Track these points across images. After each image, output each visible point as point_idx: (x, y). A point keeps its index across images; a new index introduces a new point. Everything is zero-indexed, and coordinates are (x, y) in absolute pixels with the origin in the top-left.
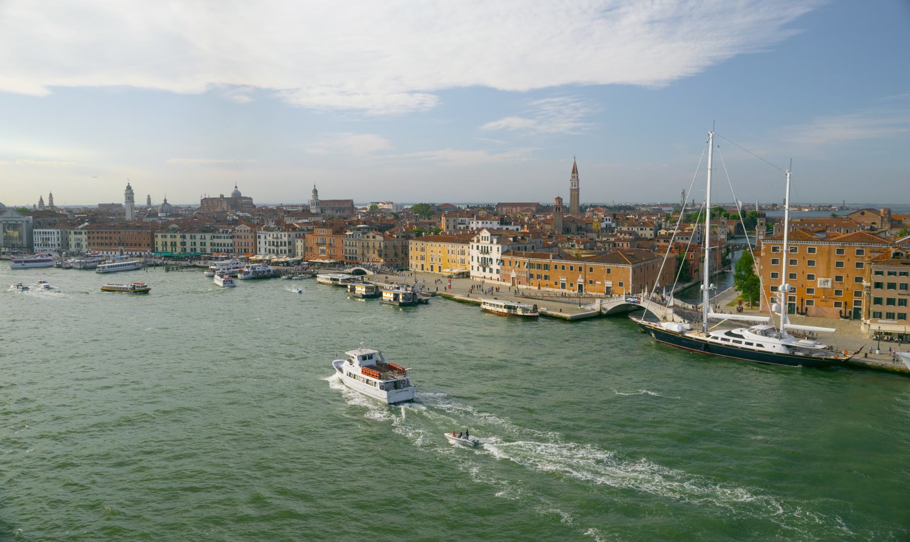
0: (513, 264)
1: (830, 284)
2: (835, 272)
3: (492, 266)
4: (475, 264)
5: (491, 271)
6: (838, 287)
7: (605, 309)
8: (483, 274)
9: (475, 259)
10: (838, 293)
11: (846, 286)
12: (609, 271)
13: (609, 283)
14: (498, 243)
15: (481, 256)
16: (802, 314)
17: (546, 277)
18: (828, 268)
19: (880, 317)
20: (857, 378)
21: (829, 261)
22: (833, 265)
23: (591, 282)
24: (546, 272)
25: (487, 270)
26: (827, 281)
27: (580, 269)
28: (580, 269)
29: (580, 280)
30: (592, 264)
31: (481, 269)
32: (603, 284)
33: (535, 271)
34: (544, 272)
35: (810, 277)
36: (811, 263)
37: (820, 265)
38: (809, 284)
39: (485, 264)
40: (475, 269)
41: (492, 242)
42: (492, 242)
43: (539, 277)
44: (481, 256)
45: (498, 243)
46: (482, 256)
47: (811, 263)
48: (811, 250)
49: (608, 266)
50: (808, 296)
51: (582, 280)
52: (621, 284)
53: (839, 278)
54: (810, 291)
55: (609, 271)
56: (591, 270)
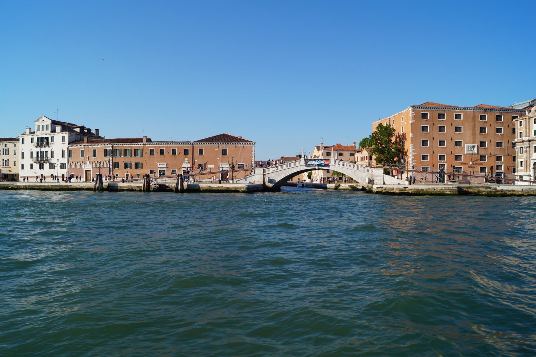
0: (86, 155)
1: (475, 149)
2: (480, 138)
3: (53, 161)
4: (28, 161)
5: (52, 166)
6: (483, 153)
7: (270, 181)
8: (39, 172)
9: (27, 155)
10: (483, 158)
11: (490, 151)
12: (225, 152)
14: (62, 131)
15: (35, 150)
17: (137, 166)
18: (474, 134)
21: (474, 127)
22: (478, 131)
24: (138, 159)
25: (46, 166)
26: (473, 147)
27: (186, 152)
28: (186, 152)
31: (36, 166)
33: (120, 160)
34: (133, 160)
35: (458, 143)
37: (466, 132)
38: (457, 151)
39: (41, 160)
40: (27, 167)
41: (53, 131)
42: (53, 131)
43: (126, 166)
44: (35, 150)
45: (62, 131)
46: (38, 149)
50: (457, 163)
53: (483, 144)
54: (458, 157)
55: (225, 152)
56: (201, 151)
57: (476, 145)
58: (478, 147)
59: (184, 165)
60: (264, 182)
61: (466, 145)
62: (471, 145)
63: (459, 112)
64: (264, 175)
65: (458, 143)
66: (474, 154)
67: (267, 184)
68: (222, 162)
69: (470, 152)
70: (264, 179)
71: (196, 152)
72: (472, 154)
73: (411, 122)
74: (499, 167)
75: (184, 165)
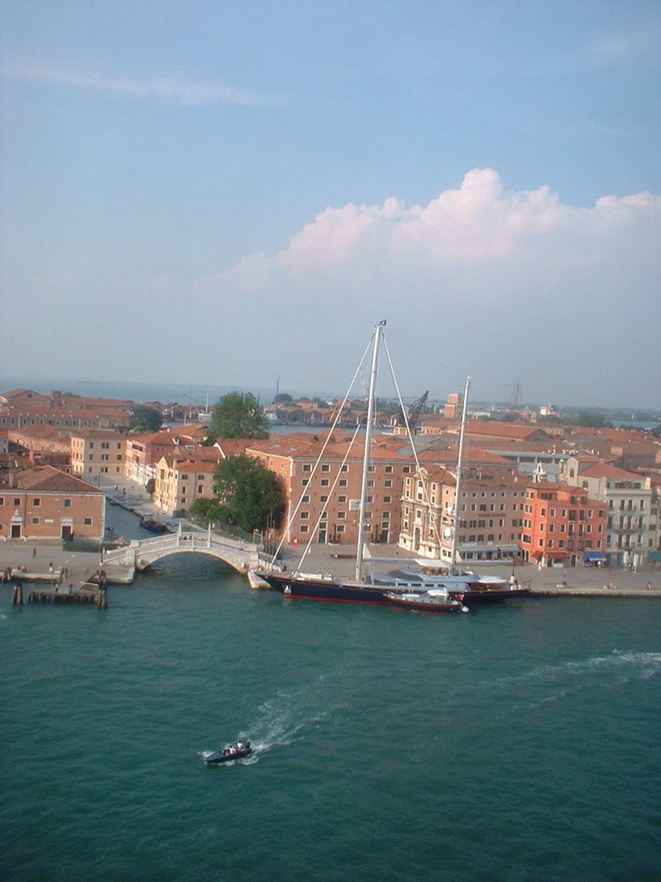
7: (143, 563)
12: (67, 503)
13: (67, 521)
16: (337, 543)
19: (464, 541)
20: (537, 603)
23: (36, 521)
28: (17, 502)
29: (17, 519)
30: (38, 494)
32: (57, 522)
49: (66, 495)
50: (339, 521)
51: (20, 519)
52: (88, 521)
56: (37, 502)
59: (13, 519)
61: (350, 501)
62: (356, 501)
64: (135, 556)
65: (342, 499)
68: (65, 514)
69: (355, 509)
70: (135, 560)
71: (31, 503)
73: (291, 475)
74: (385, 525)
75: (13, 519)
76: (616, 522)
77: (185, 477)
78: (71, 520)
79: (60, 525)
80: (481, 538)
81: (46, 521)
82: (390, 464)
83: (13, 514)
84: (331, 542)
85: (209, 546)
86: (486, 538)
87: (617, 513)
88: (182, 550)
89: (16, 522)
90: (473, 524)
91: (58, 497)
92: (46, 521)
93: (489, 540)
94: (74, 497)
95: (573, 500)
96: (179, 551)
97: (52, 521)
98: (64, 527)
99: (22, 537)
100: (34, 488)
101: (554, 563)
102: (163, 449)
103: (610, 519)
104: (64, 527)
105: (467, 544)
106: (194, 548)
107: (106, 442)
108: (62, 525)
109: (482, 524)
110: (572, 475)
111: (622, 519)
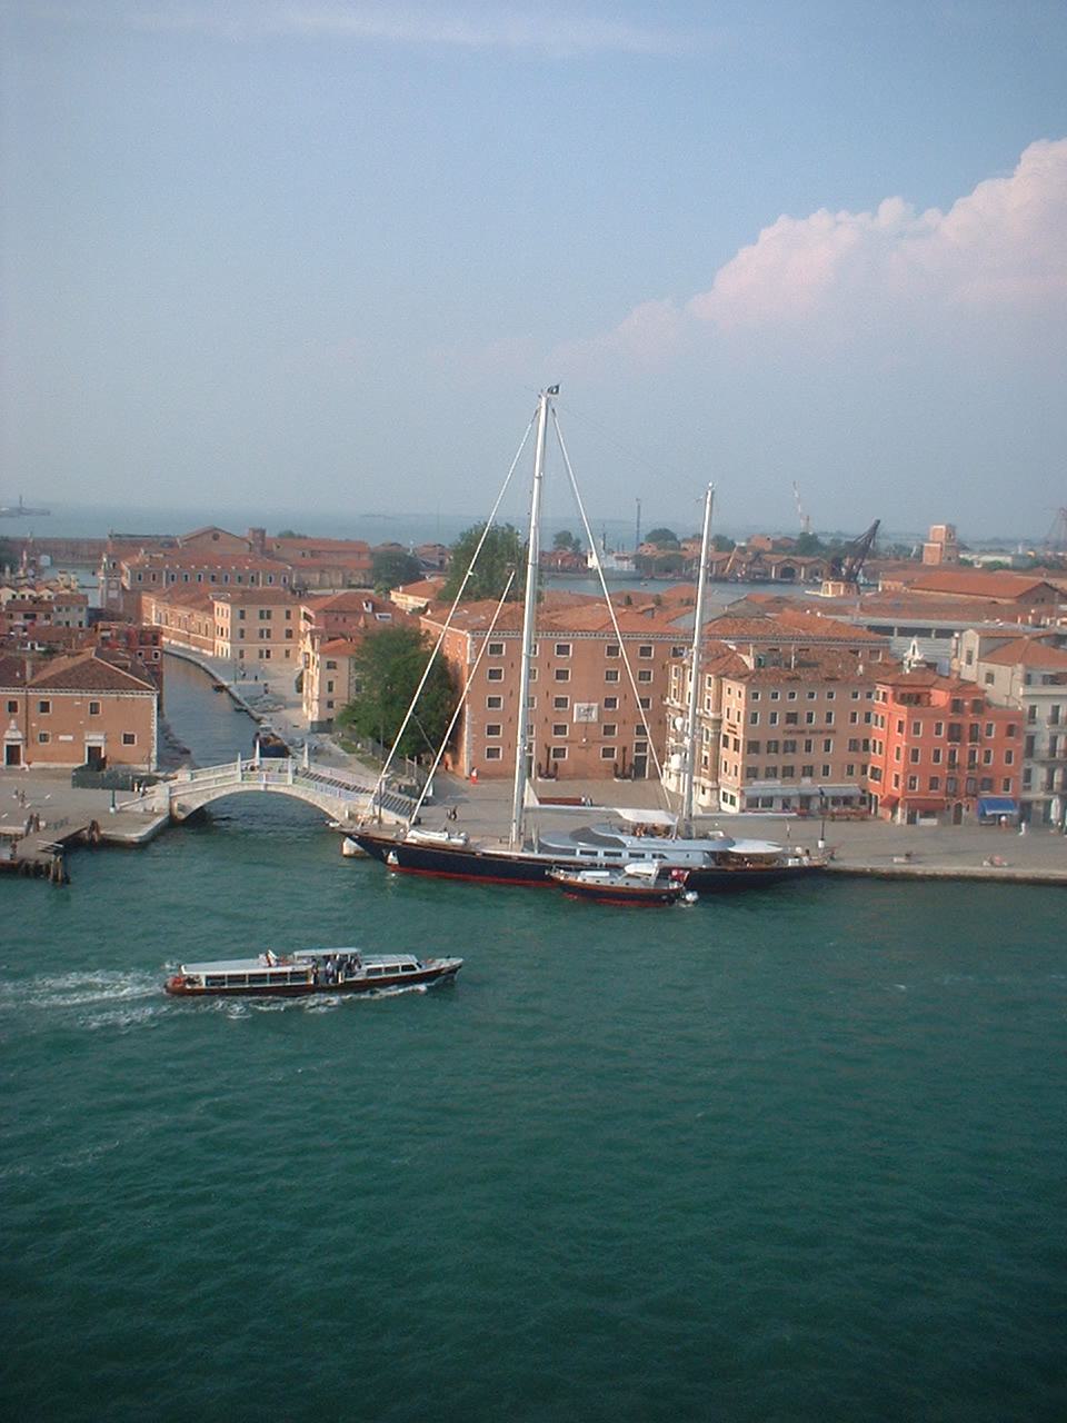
1: (594, 714)
7: (182, 808)
12: (94, 709)
13: (96, 739)
16: (550, 777)
23: (44, 738)
27: (13, 707)
28: (13, 707)
29: (13, 734)
30: (47, 694)
32: (79, 740)
35: (561, 702)
36: (562, 675)
47: (562, 675)
48: (563, 650)
50: (557, 741)
52: (129, 739)
53: (610, 703)
54: (559, 730)
55: (94, 709)
56: (45, 707)
57: (596, 705)
58: (599, 707)
60: (171, 810)
61: (575, 705)
62: (586, 705)
63: (567, 640)
64: (171, 798)
65: (561, 702)
66: (592, 723)
67: (176, 813)
69: (584, 719)
70: (171, 803)
72: (587, 723)
74: (641, 747)
76: (1043, 746)
77: (331, 666)
78: (101, 737)
79: (84, 746)
80: (788, 772)
81: (61, 738)
82: (650, 642)
83: (7, 727)
84: (541, 776)
85: (290, 782)
86: (799, 771)
87: (1043, 730)
88: (246, 788)
89: (13, 740)
90: (773, 747)
91: (80, 698)
92: (61, 738)
93: (804, 775)
94: (105, 698)
95: (956, 706)
96: (241, 789)
97: (70, 738)
98: (89, 748)
99: (23, 765)
100: (43, 685)
101: (921, 817)
102: (344, 620)
103: (1031, 740)
104: (89, 748)
105: (762, 783)
106: (266, 785)
107: (265, 608)
108: (88, 744)
109: (791, 747)
110: (969, 662)
111: (1054, 740)
